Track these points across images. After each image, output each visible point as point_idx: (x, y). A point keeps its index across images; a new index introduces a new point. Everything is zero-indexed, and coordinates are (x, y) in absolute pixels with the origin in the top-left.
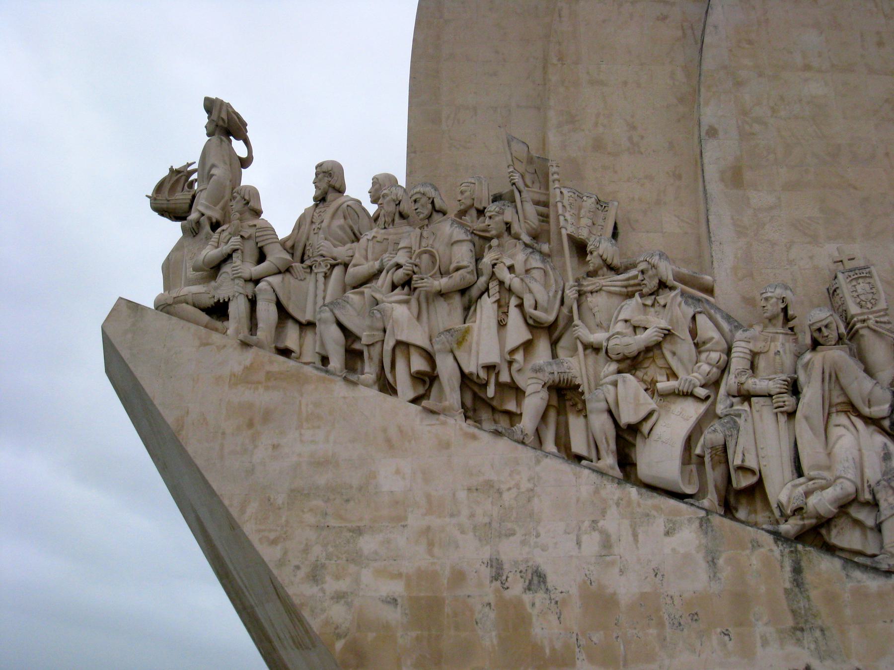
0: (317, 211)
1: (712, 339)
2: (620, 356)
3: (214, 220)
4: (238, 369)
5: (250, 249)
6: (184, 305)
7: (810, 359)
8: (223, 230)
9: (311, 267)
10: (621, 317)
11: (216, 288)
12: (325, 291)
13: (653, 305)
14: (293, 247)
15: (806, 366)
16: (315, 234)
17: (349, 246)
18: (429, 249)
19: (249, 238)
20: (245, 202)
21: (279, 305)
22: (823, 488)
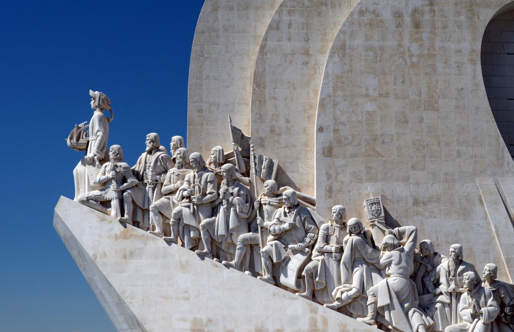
0: (148, 156)
3: (101, 159)
4: (118, 233)
5: (120, 177)
7: (348, 239)
9: (146, 183)
10: (277, 216)
11: (106, 193)
13: (289, 213)
15: (346, 242)
16: (148, 168)
17: (163, 175)
18: (198, 183)
19: (119, 172)
20: (116, 154)
21: (133, 201)
22: (348, 291)
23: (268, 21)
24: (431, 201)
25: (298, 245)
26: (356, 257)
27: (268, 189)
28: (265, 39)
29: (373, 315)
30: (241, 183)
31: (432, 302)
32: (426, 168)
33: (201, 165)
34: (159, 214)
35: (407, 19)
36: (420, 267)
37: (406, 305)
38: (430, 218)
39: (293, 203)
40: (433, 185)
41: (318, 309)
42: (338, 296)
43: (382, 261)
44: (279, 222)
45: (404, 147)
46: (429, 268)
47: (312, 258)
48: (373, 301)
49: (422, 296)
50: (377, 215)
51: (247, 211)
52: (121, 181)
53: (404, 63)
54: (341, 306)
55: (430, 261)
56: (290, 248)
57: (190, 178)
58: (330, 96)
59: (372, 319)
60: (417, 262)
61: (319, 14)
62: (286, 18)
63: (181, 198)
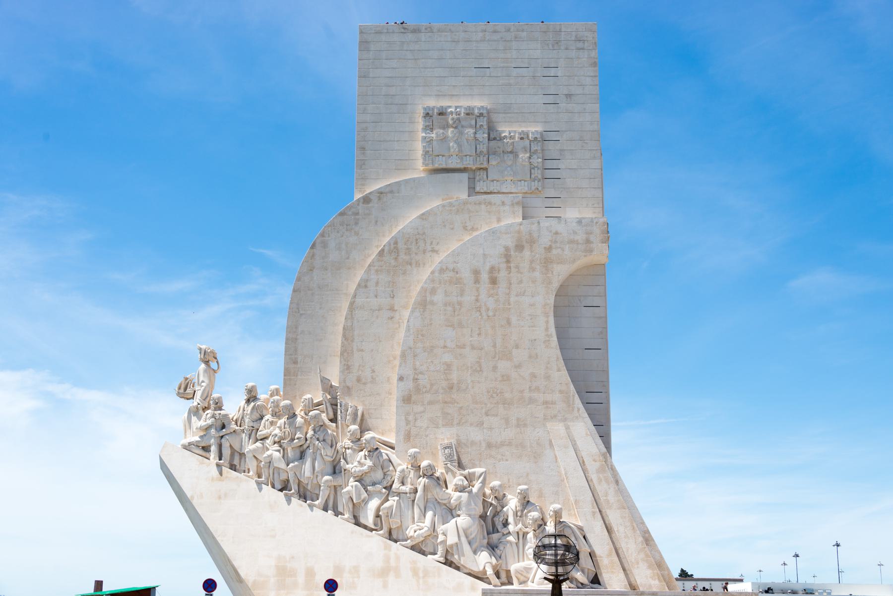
5: (219, 424)
6: (192, 446)
8: (207, 414)
10: (358, 460)
14: (236, 420)
23: (358, 279)
24: (503, 445)
26: (429, 497)
28: (355, 296)
31: (500, 541)
32: (499, 414)
34: (253, 458)
35: (485, 276)
46: (499, 508)
48: (443, 540)
49: (491, 535)
51: (331, 455)
52: (221, 427)
57: (281, 425)
58: (411, 348)
61: (404, 273)
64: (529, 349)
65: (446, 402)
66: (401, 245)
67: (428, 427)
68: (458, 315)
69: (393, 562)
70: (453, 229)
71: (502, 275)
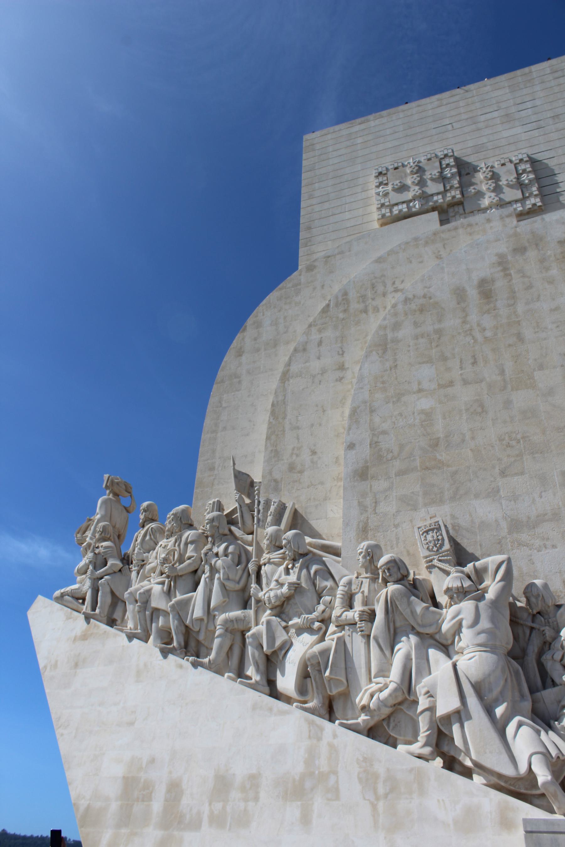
1: (326, 587)
2: (270, 606)
5: (100, 560)
6: (67, 597)
12: (136, 582)
19: (99, 553)
21: (113, 593)
22: (381, 690)
25: (302, 617)
26: (398, 624)
27: (268, 539)
28: (289, 364)
29: (428, 736)
30: (239, 542)
33: (183, 522)
35: (473, 293)
36: (530, 635)
37: (499, 711)
38: (544, 549)
39: (296, 550)
40: (543, 494)
41: (322, 729)
42: (364, 702)
43: (445, 627)
44: (279, 586)
45: (485, 446)
46: (549, 633)
47: (326, 639)
48: (427, 706)
49: (538, 694)
50: (436, 548)
51: (237, 578)
53: (473, 341)
54: (372, 723)
55: (550, 620)
56: (293, 626)
59: (426, 745)
60: (524, 627)
62: (315, 336)
63: (160, 574)
64: (562, 366)
65: (427, 468)
66: (353, 295)
67: (398, 511)
68: (437, 346)
69: (323, 764)
70: (421, 262)
71: (500, 284)
